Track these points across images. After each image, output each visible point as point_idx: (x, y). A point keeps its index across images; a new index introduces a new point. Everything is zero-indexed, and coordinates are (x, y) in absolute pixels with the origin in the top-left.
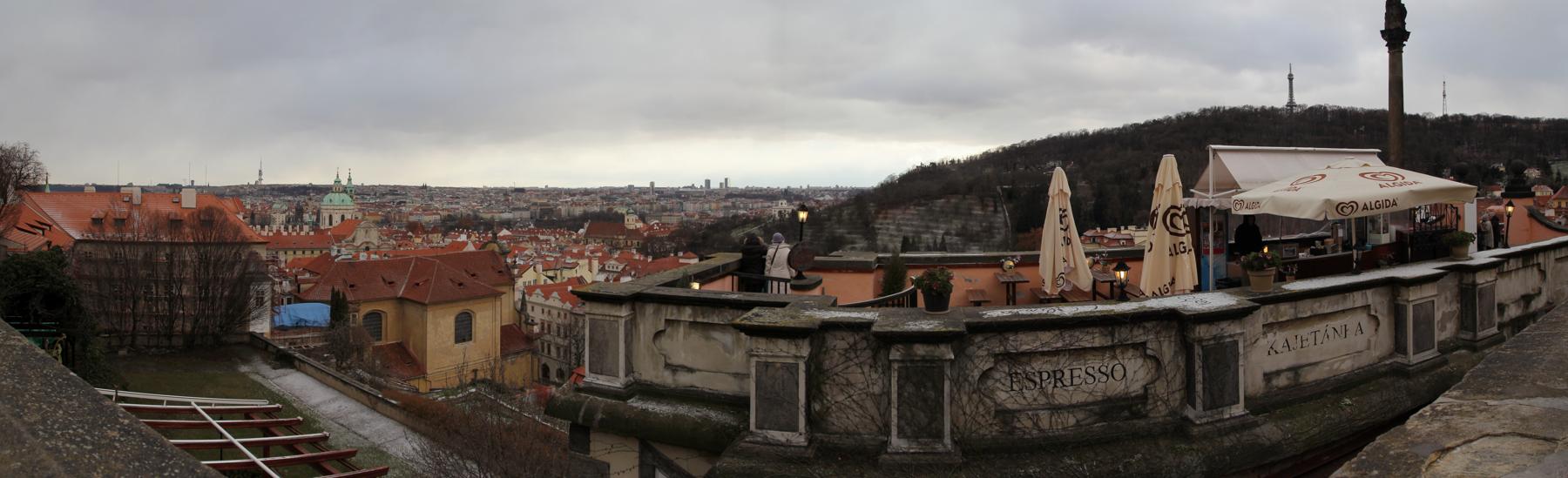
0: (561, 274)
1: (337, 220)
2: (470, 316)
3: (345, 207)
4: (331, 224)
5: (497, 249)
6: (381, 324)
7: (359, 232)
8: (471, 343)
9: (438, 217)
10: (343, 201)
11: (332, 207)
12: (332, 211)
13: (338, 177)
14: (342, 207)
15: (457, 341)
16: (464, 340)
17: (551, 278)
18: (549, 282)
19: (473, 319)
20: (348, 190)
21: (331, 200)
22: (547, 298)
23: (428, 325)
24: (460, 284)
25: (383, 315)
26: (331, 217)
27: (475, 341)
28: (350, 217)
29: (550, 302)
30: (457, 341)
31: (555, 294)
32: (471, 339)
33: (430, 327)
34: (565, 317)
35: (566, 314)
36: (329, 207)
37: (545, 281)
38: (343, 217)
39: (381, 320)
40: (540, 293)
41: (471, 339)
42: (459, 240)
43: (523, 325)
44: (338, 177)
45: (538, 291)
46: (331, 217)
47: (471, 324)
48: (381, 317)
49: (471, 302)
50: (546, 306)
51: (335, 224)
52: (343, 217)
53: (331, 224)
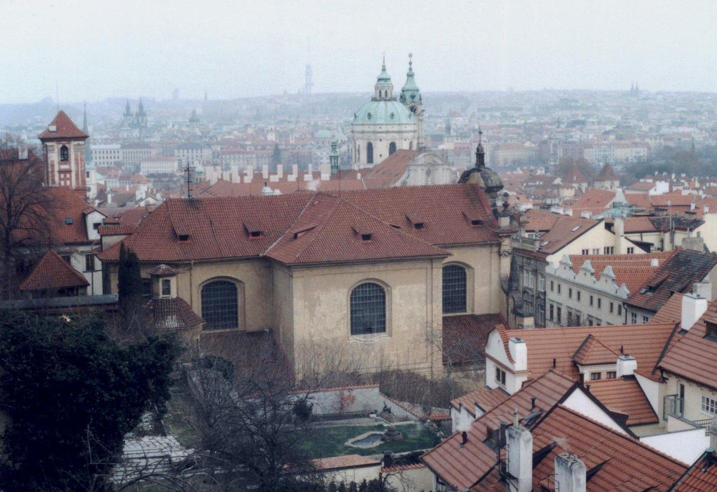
0: (672, 241)
1: (381, 151)
2: (382, 290)
3: (396, 128)
4: (370, 159)
5: (482, 184)
6: (236, 300)
7: (412, 174)
8: (383, 335)
9: (643, 152)
10: (392, 115)
11: (372, 129)
12: (372, 135)
13: (384, 70)
14: (390, 128)
15: (354, 331)
16: (369, 330)
17: (646, 246)
18: (638, 251)
19: (387, 296)
20: (408, 95)
21: (369, 115)
22: (597, 275)
23: (295, 300)
24: (366, 237)
25: (237, 285)
26: (370, 147)
27: (390, 335)
28: (405, 146)
29: (602, 285)
30: (354, 331)
31: (609, 270)
32: (384, 330)
33: (298, 304)
34: (620, 313)
35: (620, 306)
36: (366, 129)
37: (630, 250)
38: (393, 146)
39: (236, 295)
40: (590, 267)
41: (384, 330)
42: (652, 192)
43: (511, 316)
44: (384, 70)
45: (587, 264)
46: (370, 147)
47: (384, 303)
48: (236, 289)
49: (382, 267)
50: (600, 292)
51: (377, 160)
52: (393, 146)
53: (370, 159)
